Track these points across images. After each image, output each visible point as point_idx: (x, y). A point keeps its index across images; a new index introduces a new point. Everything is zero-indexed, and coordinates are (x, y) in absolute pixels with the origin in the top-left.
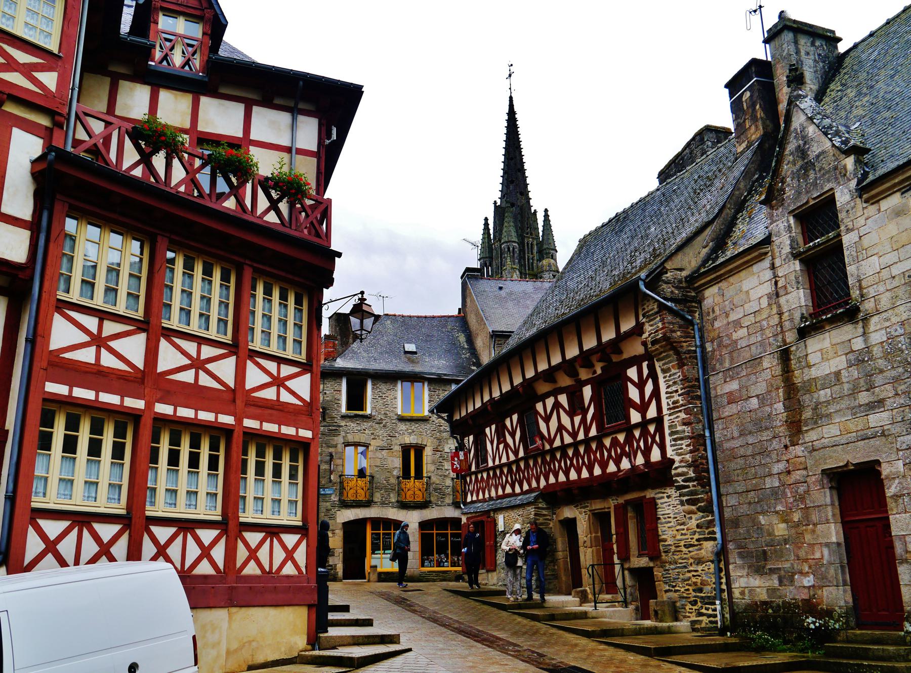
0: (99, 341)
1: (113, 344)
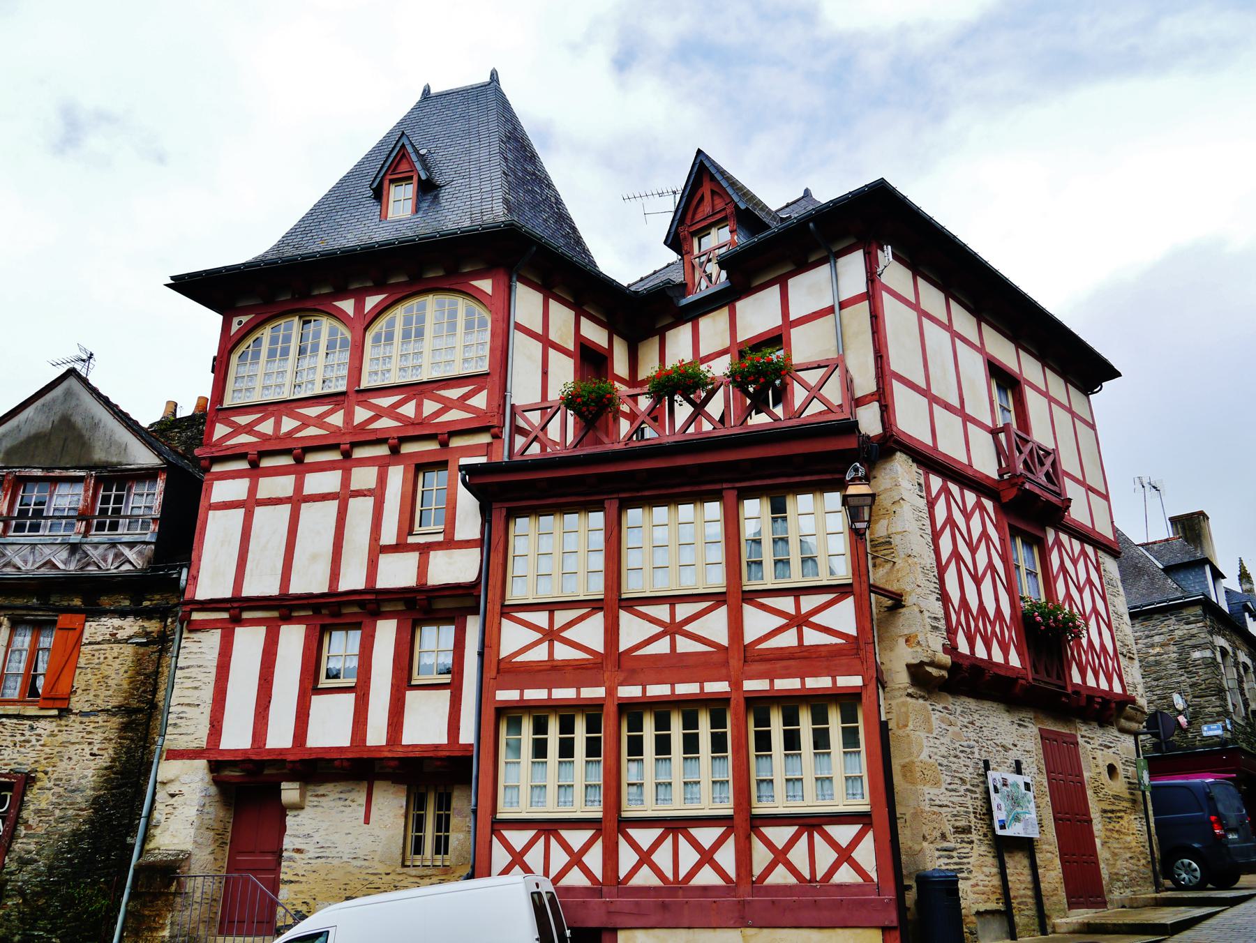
1: (565, 634)
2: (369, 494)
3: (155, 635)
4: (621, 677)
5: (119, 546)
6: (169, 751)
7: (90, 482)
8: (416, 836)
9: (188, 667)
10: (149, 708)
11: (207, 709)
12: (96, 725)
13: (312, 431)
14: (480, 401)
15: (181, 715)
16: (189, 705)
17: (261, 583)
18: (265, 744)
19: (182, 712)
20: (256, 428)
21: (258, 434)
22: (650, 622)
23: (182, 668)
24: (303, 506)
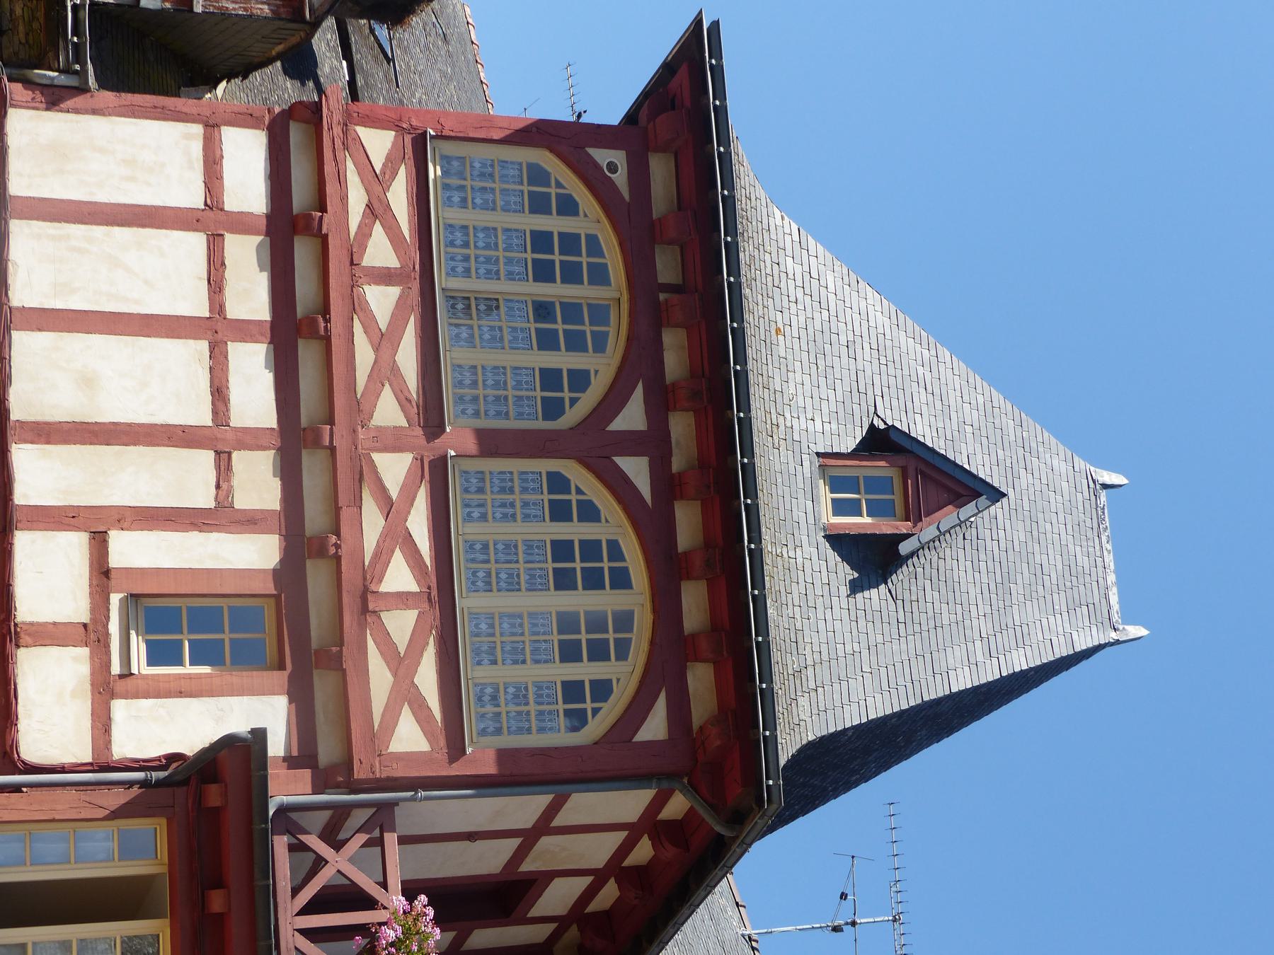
2: (222, 493)
13: (364, 355)
20: (378, 228)
21: (365, 233)
24: (203, 346)
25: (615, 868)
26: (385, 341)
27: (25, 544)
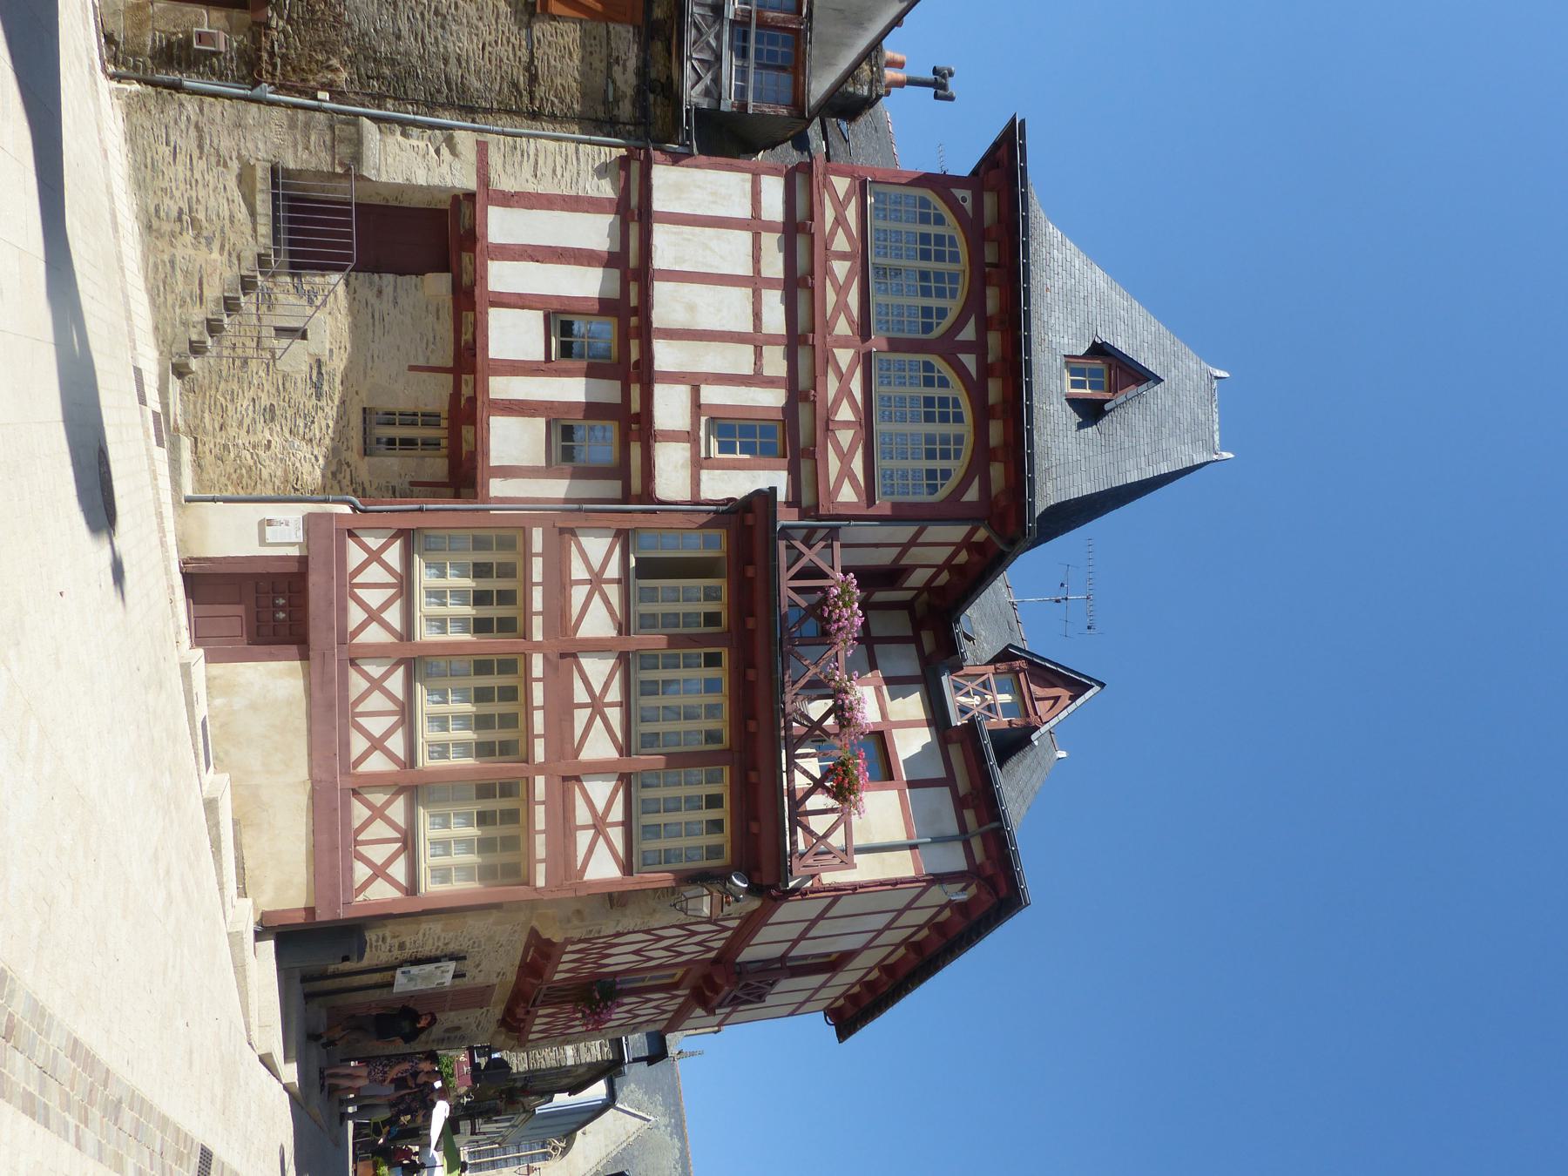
0: (596, 581)
1: (597, 598)
2: (757, 367)
3: (615, 112)
4: (554, 657)
5: (717, 66)
6: (485, 144)
7: (794, 23)
8: (400, 445)
9: (578, 159)
10: (533, 110)
11: (531, 187)
12: (517, 49)
13: (831, 297)
14: (847, 494)
15: (525, 155)
16: (536, 163)
17: (668, 247)
18: (492, 259)
19: (528, 154)
20: (840, 230)
21: (833, 233)
22: (605, 683)
23: (577, 150)
24: (749, 291)
25: (948, 565)
26: (842, 290)
27: (659, 390)
